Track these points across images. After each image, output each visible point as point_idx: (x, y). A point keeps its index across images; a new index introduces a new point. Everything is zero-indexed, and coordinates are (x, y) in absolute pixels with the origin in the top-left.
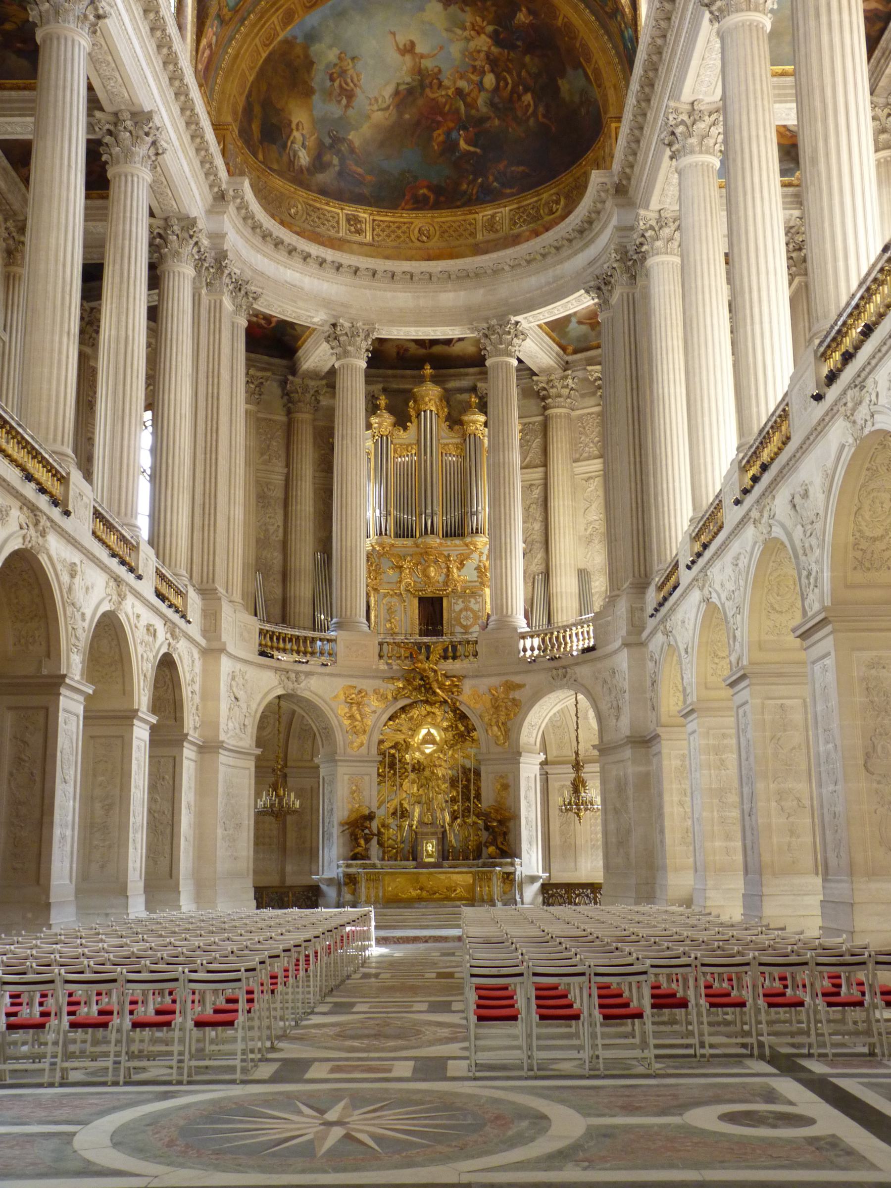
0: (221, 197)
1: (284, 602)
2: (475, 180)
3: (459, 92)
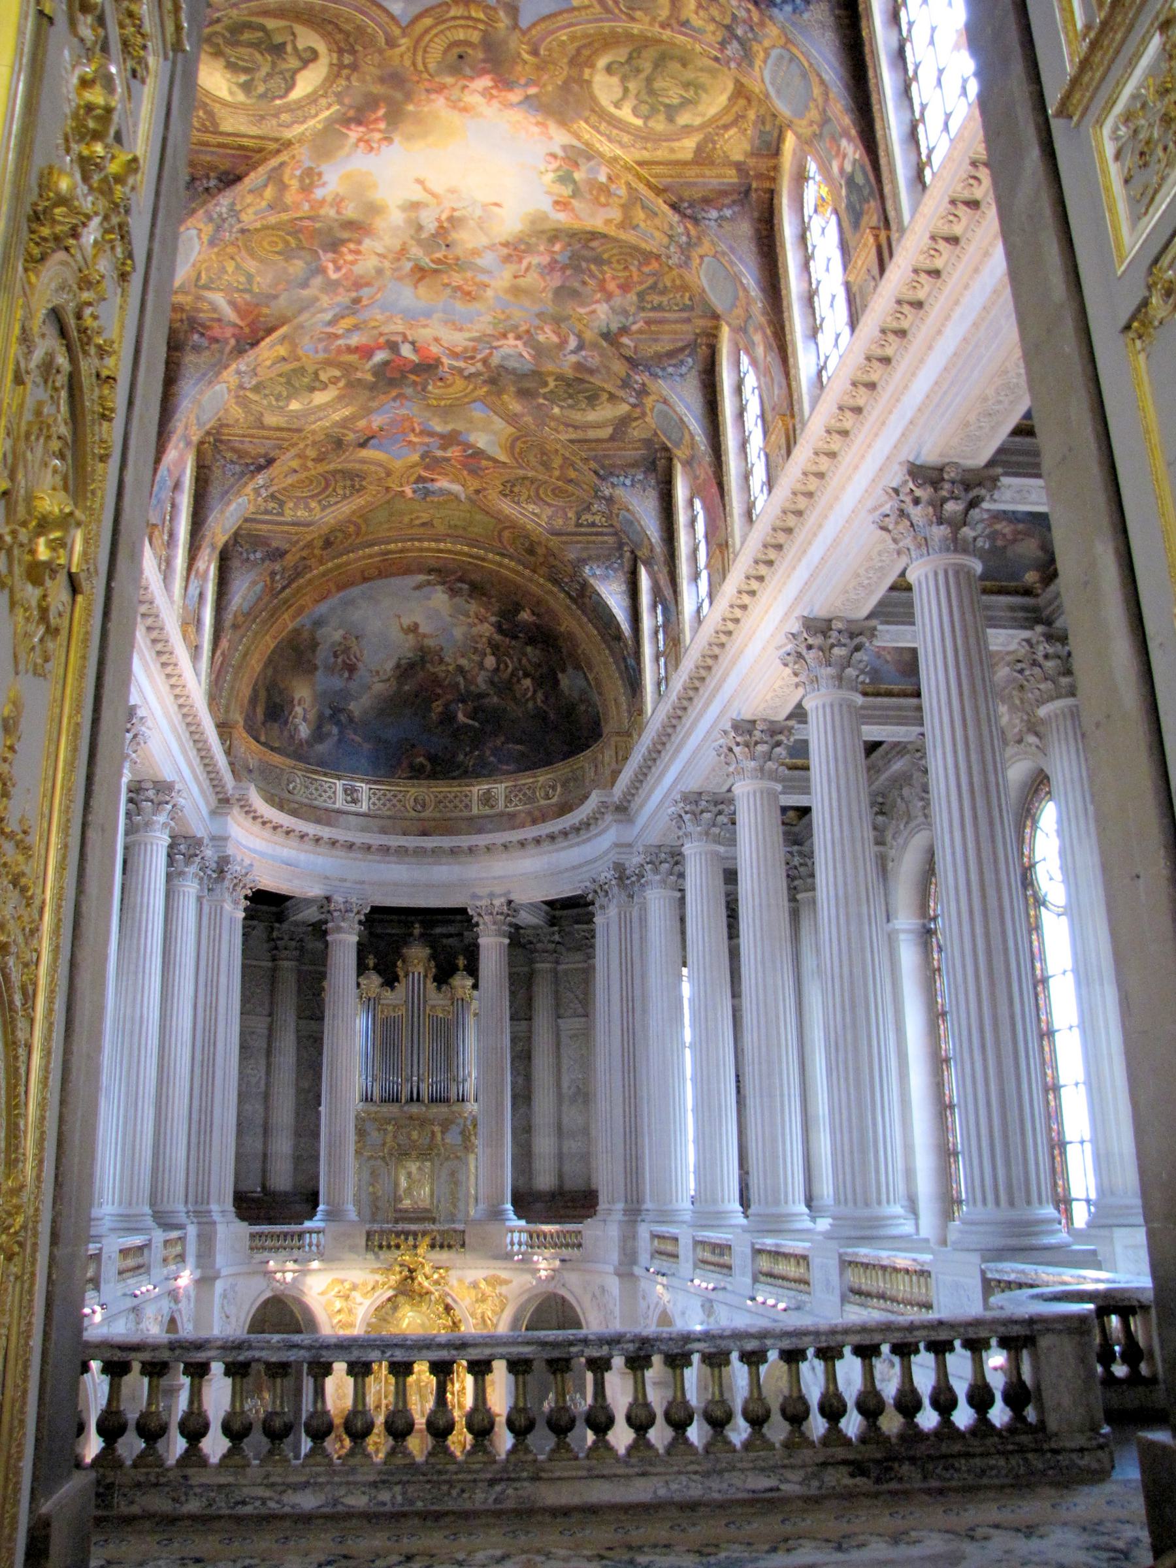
0: (225, 801)
1: (265, 1155)
2: (471, 752)
3: (460, 669)
